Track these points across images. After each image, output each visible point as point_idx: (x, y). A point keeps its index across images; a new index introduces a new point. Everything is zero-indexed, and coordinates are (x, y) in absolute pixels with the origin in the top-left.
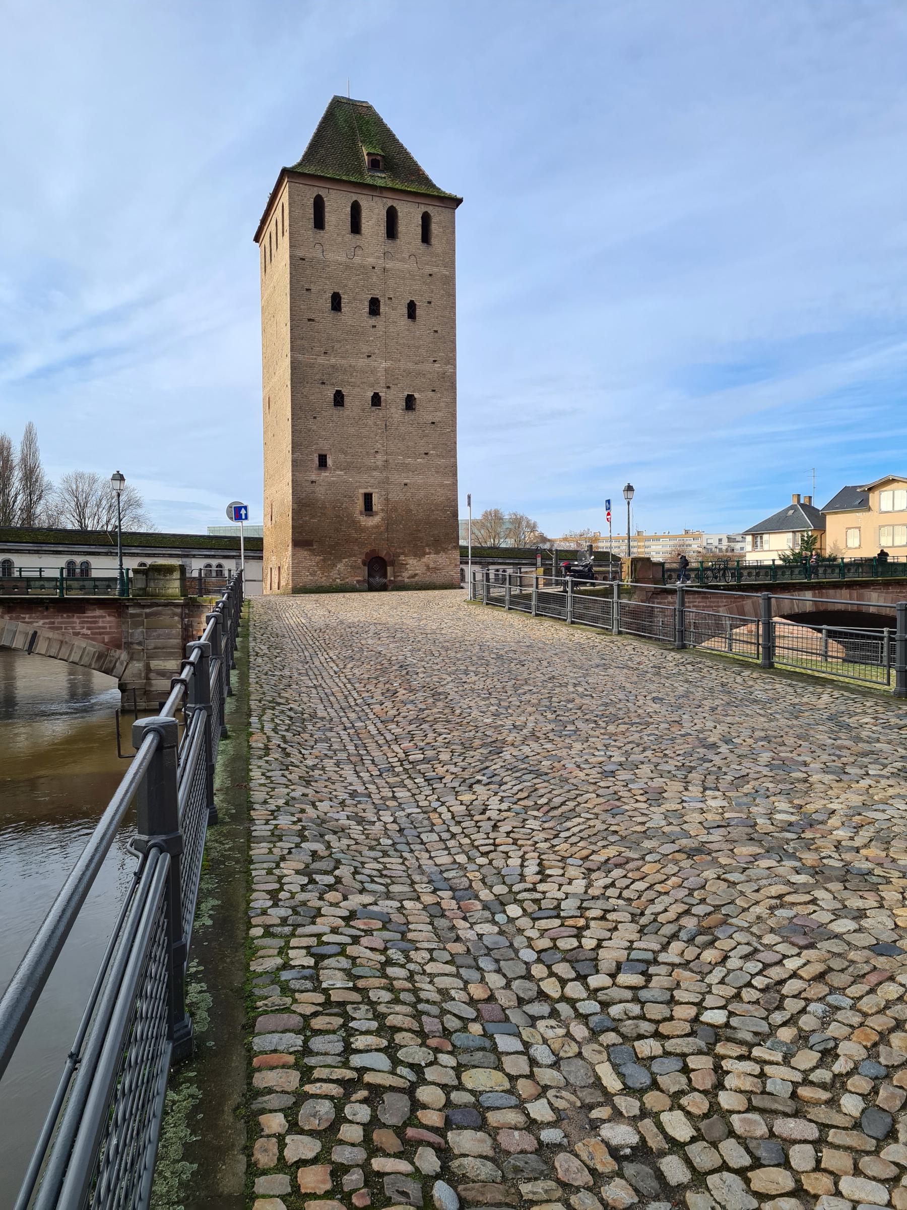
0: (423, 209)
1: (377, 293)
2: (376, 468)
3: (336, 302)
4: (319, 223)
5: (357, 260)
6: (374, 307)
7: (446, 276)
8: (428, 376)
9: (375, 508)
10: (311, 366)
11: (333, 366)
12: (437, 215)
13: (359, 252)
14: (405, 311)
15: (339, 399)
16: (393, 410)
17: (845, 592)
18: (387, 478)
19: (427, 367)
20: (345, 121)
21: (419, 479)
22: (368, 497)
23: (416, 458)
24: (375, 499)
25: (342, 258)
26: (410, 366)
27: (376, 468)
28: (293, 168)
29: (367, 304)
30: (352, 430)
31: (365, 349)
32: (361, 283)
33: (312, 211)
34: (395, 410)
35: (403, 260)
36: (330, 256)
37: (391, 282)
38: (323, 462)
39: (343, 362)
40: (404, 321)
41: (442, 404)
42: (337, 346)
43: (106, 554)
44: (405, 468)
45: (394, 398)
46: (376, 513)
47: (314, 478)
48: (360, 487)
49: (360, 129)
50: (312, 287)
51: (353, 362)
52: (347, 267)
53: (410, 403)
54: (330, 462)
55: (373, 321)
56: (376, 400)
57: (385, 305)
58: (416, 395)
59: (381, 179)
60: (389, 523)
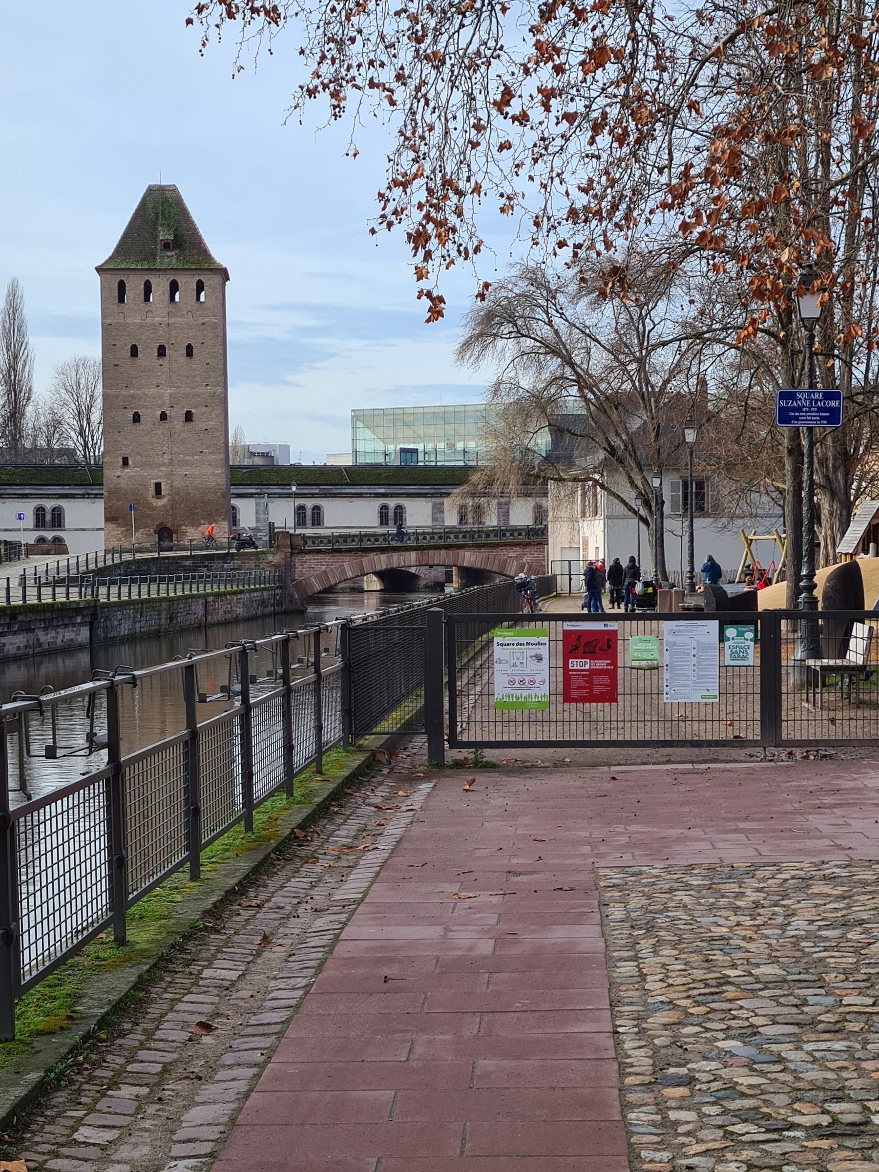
0: (197, 278)
1: (163, 342)
2: (164, 465)
3: (134, 352)
4: (121, 300)
5: (149, 320)
6: (162, 351)
7: (215, 323)
8: (202, 396)
9: (163, 493)
10: (117, 397)
11: (132, 396)
12: (210, 281)
13: (150, 314)
14: (185, 352)
15: (137, 418)
16: (176, 423)
17: (443, 552)
18: (172, 471)
19: (201, 390)
20: (154, 208)
21: (196, 471)
22: (158, 486)
23: (193, 456)
24: (163, 487)
25: (138, 320)
26: (188, 390)
27: (164, 465)
28: (103, 265)
29: (156, 350)
30: (146, 439)
31: (155, 382)
32: (152, 336)
33: (117, 291)
34: (178, 423)
35: (182, 316)
36: (129, 320)
37: (174, 333)
38: (125, 462)
39: (139, 392)
40: (184, 359)
41: (213, 416)
42: (135, 381)
43: (83, 496)
44: (186, 463)
45: (177, 415)
46: (164, 497)
47: (119, 474)
48: (151, 479)
49: (163, 213)
50: (117, 343)
51: (146, 391)
52: (142, 326)
53: (189, 417)
54: (130, 462)
55: (160, 362)
56: (164, 416)
57: (169, 349)
58: (193, 411)
59: (170, 258)
60: (173, 504)
